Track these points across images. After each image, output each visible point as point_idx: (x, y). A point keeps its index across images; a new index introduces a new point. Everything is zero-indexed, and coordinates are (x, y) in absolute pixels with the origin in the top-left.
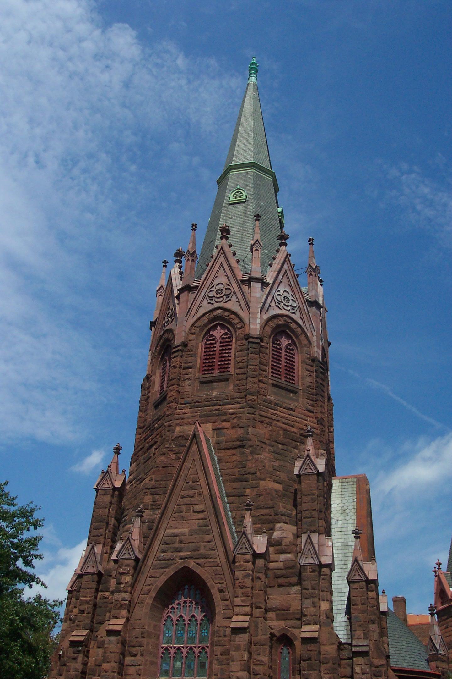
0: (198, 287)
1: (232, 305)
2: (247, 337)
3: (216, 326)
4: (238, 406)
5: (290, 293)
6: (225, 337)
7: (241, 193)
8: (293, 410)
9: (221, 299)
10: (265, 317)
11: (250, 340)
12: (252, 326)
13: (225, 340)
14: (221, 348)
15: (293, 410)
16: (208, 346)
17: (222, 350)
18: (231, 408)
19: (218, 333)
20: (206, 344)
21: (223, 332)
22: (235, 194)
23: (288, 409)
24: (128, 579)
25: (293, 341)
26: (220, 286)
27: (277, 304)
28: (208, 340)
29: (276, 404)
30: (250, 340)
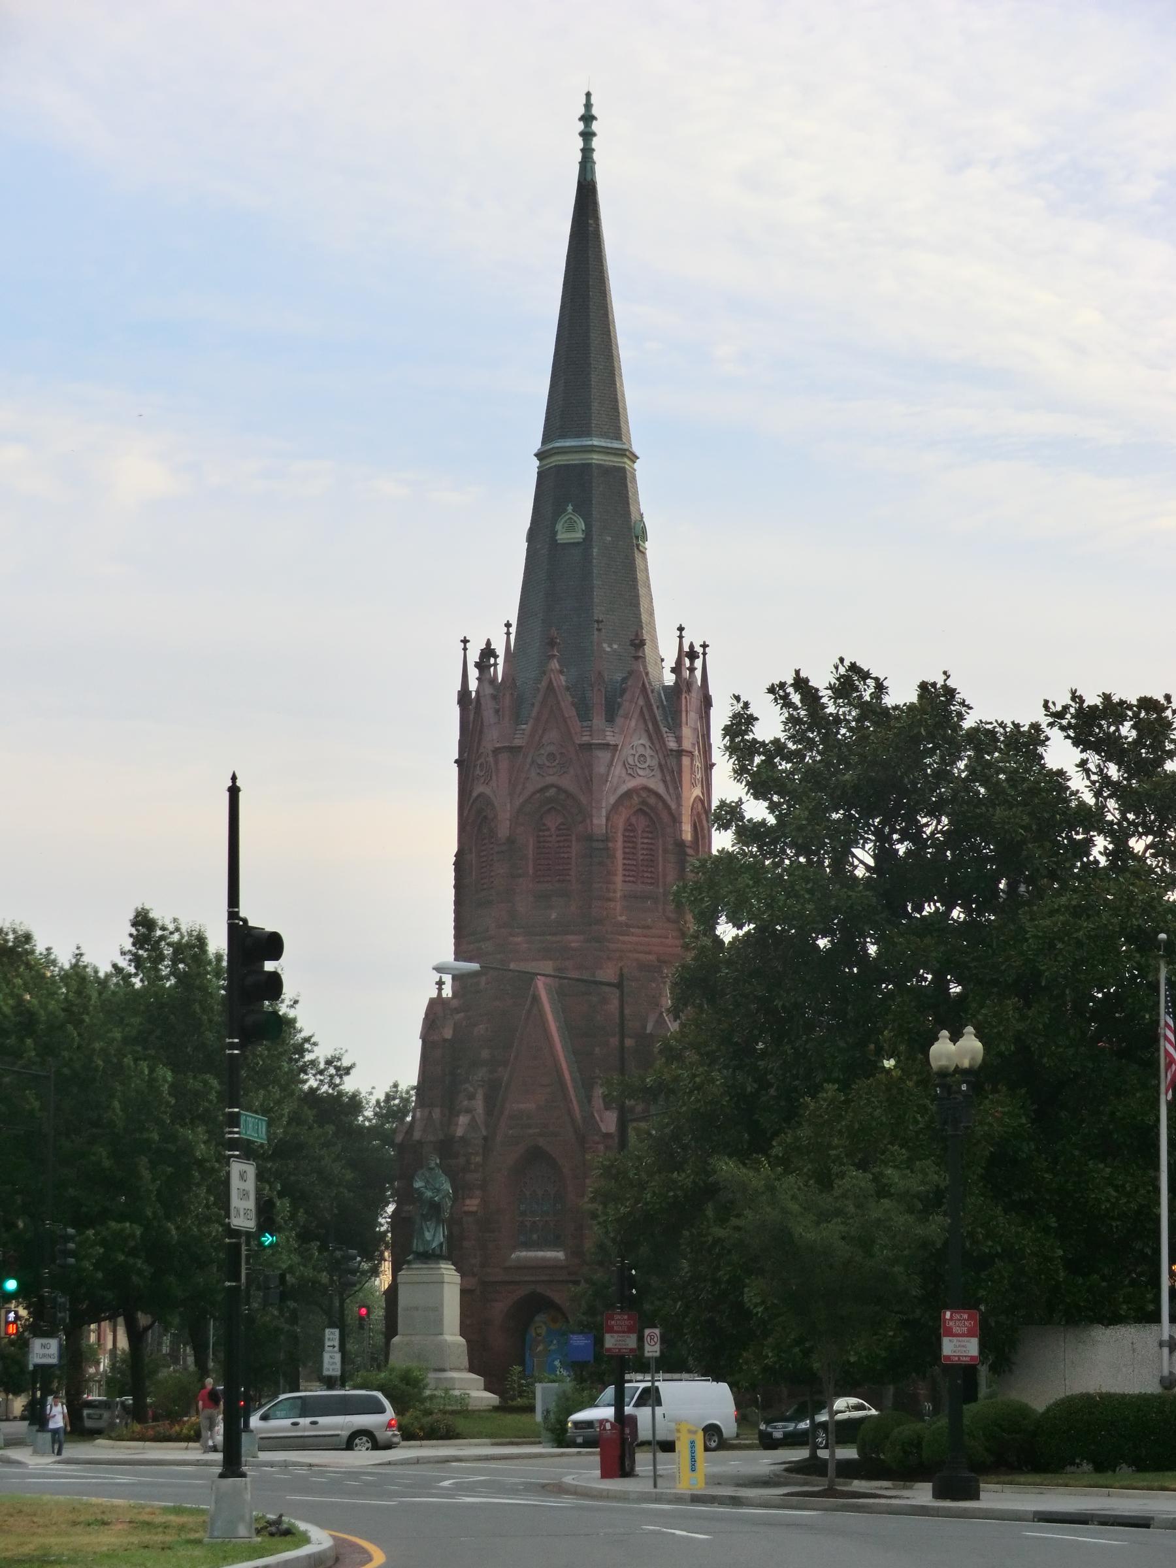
0: (520, 747)
1: (567, 782)
2: (590, 838)
3: (549, 810)
4: (581, 937)
5: (648, 744)
6: (562, 827)
7: (575, 522)
8: (648, 927)
9: (555, 770)
10: (612, 800)
11: (595, 845)
12: (595, 821)
13: (561, 832)
14: (557, 845)
15: (648, 927)
16: (542, 839)
17: (559, 847)
18: (574, 941)
19: (552, 822)
20: (538, 836)
21: (560, 820)
22: (566, 522)
23: (644, 927)
24: (478, 1159)
25: (651, 818)
26: (551, 749)
27: (630, 771)
28: (541, 831)
29: (627, 925)
30: (595, 845)
